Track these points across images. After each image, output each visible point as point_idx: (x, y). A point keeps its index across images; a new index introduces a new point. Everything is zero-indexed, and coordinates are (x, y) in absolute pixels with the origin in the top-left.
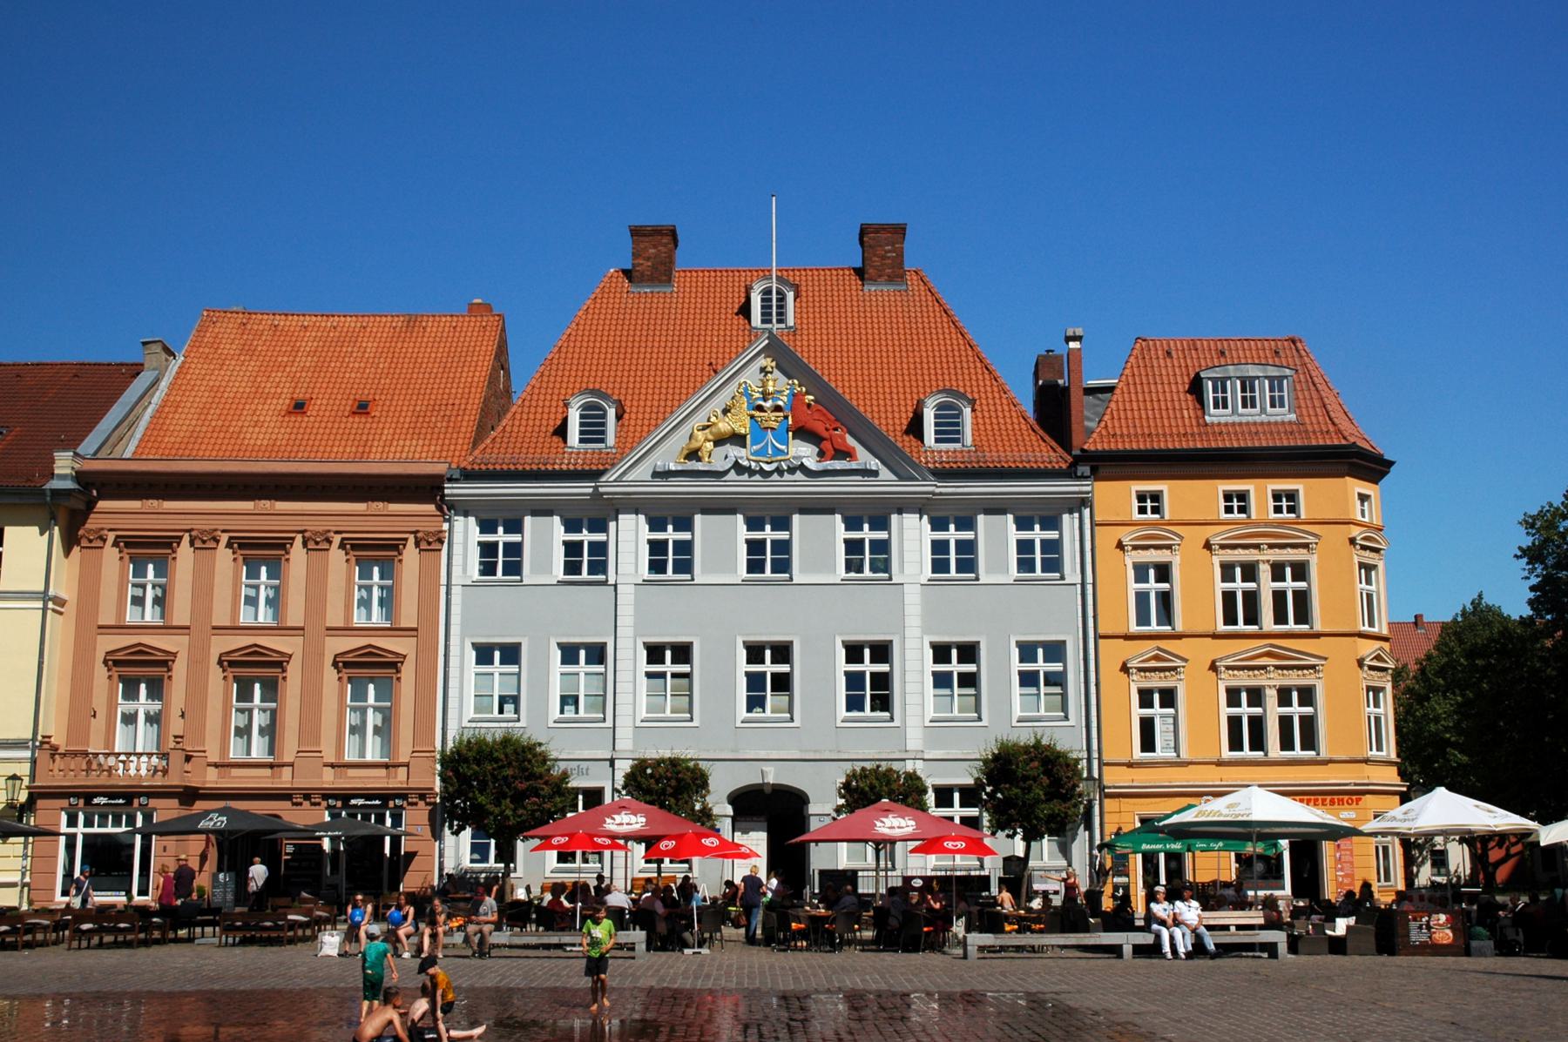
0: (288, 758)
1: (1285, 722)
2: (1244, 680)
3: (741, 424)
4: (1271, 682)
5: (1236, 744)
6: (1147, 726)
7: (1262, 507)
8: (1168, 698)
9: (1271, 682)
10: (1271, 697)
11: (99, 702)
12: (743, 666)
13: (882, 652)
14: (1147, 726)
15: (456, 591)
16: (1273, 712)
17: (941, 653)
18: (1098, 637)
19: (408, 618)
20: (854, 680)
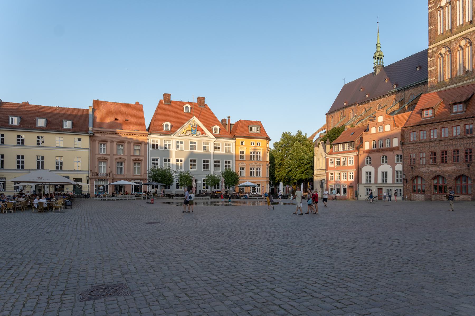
0: (126, 174)
1: (257, 172)
2: (252, 167)
3: (190, 129)
4: (256, 167)
5: (251, 175)
6: (241, 172)
7: (256, 144)
8: (243, 169)
9: (256, 167)
10: (255, 169)
11: (96, 165)
12: (190, 163)
13: (208, 162)
14: (241, 172)
15: (149, 151)
16: (255, 171)
17: (215, 162)
18: (235, 160)
19: (143, 155)
20: (204, 165)
